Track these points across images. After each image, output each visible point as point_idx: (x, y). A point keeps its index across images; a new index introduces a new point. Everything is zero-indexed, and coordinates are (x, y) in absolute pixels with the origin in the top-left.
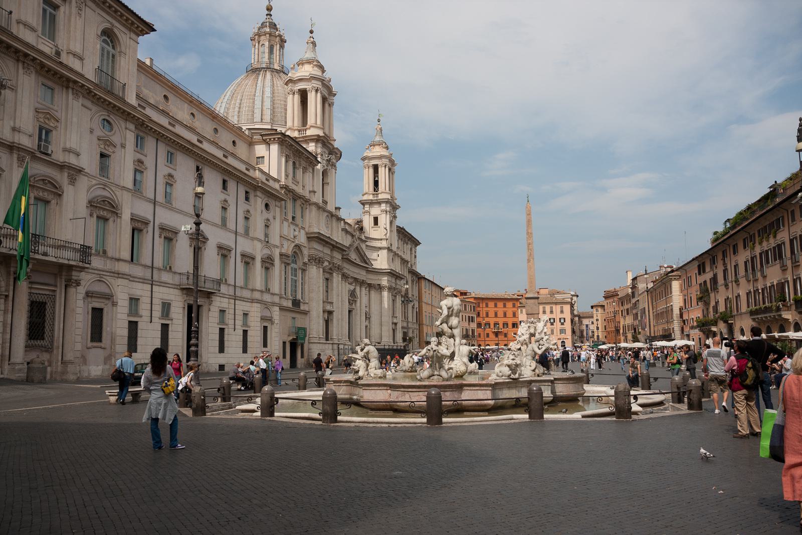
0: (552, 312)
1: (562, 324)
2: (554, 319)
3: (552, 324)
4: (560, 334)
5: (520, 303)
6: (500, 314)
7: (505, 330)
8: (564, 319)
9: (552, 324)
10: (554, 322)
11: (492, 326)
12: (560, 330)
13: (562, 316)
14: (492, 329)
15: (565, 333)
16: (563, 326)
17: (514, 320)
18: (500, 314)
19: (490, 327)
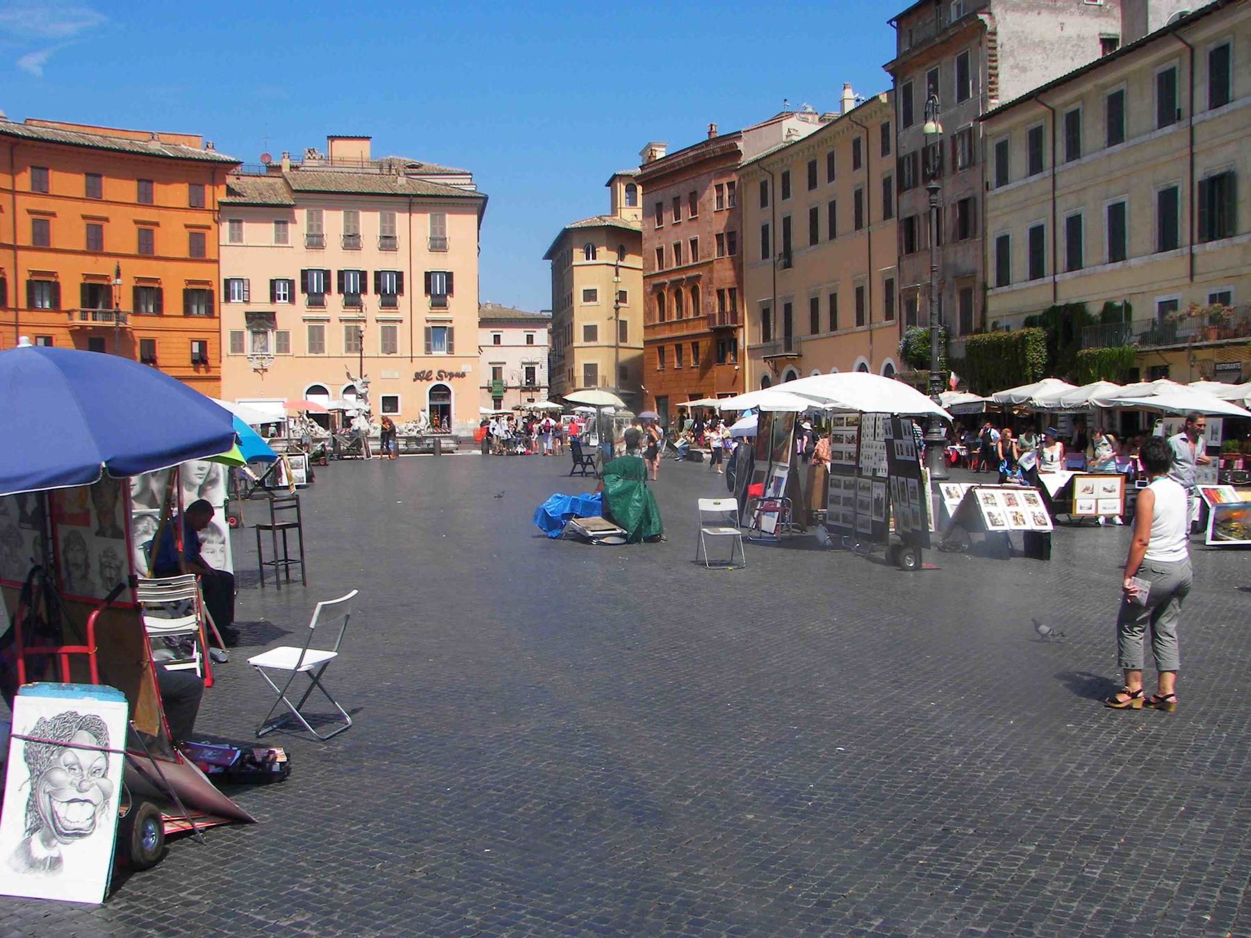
0: (388, 242)
1: (439, 302)
2: (400, 275)
3: (389, 302)
4: (428, 349)
5: (230, 192)
6: (121, 235)
7: (141, 326)
8: (449, 276)
9: (389, 302)
10: (400, 289)
11: (71, 297)
12: (427, 329)
13: (438, 263)
14: (70, 312)
15: (451, 348)
16: (439, 314)
17: (199, 272)
18: (121, 235)
19: (56, 306)
